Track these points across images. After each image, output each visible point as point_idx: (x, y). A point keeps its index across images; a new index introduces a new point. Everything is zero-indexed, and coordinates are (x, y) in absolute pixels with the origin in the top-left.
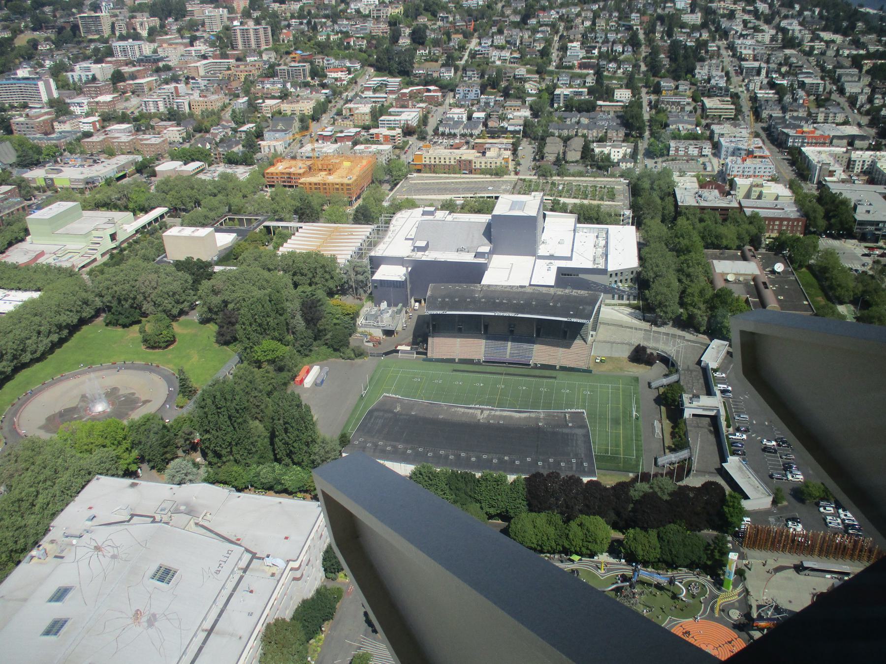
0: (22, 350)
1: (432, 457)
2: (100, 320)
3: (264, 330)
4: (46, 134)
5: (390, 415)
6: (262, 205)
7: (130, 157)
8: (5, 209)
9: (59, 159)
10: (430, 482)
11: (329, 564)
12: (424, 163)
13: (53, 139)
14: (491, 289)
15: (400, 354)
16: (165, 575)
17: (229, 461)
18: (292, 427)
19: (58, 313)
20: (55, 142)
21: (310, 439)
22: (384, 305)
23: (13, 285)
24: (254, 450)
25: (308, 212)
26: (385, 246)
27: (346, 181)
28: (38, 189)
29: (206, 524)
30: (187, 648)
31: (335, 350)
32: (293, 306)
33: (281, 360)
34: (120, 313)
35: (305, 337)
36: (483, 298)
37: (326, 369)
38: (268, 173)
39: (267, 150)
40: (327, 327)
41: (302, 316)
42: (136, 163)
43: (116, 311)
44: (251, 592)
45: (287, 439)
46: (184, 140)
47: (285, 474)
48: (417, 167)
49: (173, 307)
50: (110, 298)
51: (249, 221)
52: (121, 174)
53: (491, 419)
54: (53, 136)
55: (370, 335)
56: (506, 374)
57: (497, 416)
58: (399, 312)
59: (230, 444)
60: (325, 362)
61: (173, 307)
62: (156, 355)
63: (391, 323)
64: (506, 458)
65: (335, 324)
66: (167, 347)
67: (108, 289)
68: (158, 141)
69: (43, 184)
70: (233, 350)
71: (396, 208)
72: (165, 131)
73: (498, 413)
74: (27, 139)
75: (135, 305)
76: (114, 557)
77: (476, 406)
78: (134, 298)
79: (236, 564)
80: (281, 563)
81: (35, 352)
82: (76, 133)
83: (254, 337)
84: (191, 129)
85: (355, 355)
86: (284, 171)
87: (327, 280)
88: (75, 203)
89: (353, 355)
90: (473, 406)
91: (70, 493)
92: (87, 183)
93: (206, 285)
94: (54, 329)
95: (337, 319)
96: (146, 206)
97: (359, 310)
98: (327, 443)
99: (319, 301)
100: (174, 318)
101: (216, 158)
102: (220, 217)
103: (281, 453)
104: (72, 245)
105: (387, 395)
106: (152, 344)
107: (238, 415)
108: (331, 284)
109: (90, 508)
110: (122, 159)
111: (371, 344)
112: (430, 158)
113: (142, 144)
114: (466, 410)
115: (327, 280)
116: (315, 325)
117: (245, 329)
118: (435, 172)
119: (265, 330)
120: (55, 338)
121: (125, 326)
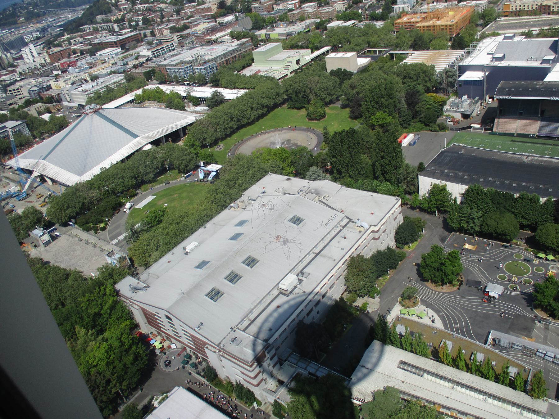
0: (242, 117)
1: (483, 181)
2: (285, 106)
3: (379, 107)
4: (269, 12)
5: (456, 155)
6: (390, 40)
7: (313, 20)
8: (243, 49)
9: (274, 25)
10: (478, 197)
11: (398, 237)
12: (511, 10)
13: (272, 14)
14: (550, 83)
15: (472, 130)
16: (297, 220)
17: (346, 176)
18: (387, 155)
19: (262, 98)
20: (273, 15)
21: (398, 164)
22: (465, 97)
23: (243, 86)
24: (362, 173)
25: (419, 43)
26: (472, 59)
27: (449, 23)
28: (261, 41)
29: (325, 201)
30: (303, 259)
31: (426, 125)
32: (401, 95)
33: (388, 126)
34: (296, 101)
35: (406, 115)
36: (542, 88)
37: (419, 136)
38: (396, 23)
39: (398, 9)
40: (422, 109)
41: (405, 101)
42: (316, 23)
43: (294, 99)
44: (345, 238)
45: (383, 163)
46: (346, 9)
47: (379, 186)
48: (506, 14)
49: (327, 97)
50: (291, 92)
51: (380, 52)
52: (307, 30)
53: (534, 162)
54: (272, 12)
55: (452, 117)
56: (554, 145)
57: (539, 160)
58: (476, 102)
59: (348, 164)
60: (418, 132)
61: (327, 97)
62: (313, 124)
63: (468, 109)
64: (541, 186)
65: (428, 108)
66: (320, 119)
67: (291, 86)
68: (330, 10)
69: (264, 37)
70: (359, 122)
71: (483, 37)
72: (335, 5)
73: (540, 159)
74: (259, 15)
75: (305, 96)
76: (271, 209)
77: (524, 154)
78: (305, 92)
79: (339, 222)
80: (366, 226)
81: (249, 119)
82: (285, 10)
83: (372, 109)
84: (351, 2)
85: (439, 128)
86: (407, 21)
87: (426, 82)
88: (279, 43)
89: (438, 129)
90: (521, 153)
91: (255, 179)
92: (288, 35)
93: (347, 83)
94: (260, 106)
95: (430, 105)
96: (319, 45)
97: (447, 100)
98: (409, 167)
99: (419, 92)
100: (327, 104)
101: (365, 18)
102: (362, 50)
103: (379, 173)
104: (275, 67)
105: (456, 144)
106: (311, 117)
107: (354, 147)
108: (429, 84)
109: (264, 188)
110: (308, 22)
111: (452, 123)
112: (516, 6)
113: (320, 13)
114: (515, 156)
115: (426, 82)
116: (414, 107)
117: (366, 105)
118: (519, 16)
119: (380, 106)
120: (260, 112)
121: (298, 109)
